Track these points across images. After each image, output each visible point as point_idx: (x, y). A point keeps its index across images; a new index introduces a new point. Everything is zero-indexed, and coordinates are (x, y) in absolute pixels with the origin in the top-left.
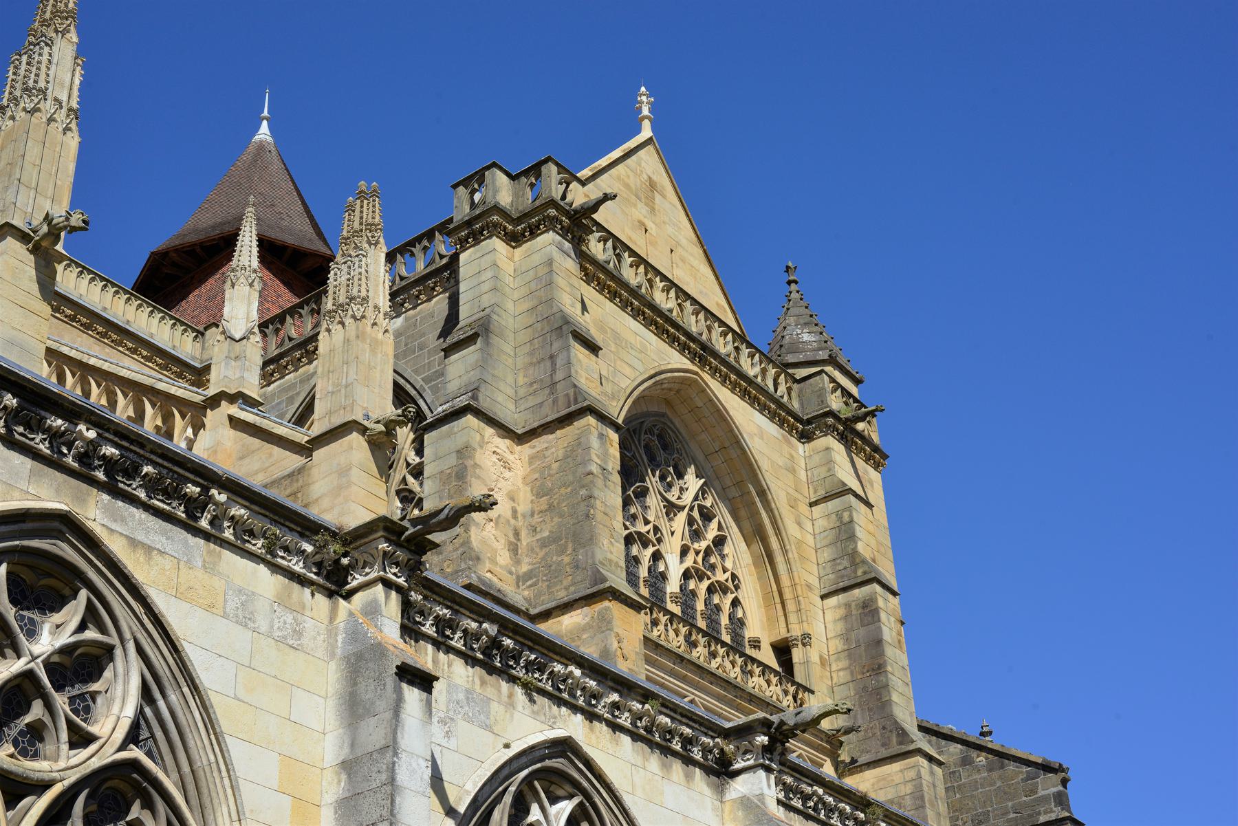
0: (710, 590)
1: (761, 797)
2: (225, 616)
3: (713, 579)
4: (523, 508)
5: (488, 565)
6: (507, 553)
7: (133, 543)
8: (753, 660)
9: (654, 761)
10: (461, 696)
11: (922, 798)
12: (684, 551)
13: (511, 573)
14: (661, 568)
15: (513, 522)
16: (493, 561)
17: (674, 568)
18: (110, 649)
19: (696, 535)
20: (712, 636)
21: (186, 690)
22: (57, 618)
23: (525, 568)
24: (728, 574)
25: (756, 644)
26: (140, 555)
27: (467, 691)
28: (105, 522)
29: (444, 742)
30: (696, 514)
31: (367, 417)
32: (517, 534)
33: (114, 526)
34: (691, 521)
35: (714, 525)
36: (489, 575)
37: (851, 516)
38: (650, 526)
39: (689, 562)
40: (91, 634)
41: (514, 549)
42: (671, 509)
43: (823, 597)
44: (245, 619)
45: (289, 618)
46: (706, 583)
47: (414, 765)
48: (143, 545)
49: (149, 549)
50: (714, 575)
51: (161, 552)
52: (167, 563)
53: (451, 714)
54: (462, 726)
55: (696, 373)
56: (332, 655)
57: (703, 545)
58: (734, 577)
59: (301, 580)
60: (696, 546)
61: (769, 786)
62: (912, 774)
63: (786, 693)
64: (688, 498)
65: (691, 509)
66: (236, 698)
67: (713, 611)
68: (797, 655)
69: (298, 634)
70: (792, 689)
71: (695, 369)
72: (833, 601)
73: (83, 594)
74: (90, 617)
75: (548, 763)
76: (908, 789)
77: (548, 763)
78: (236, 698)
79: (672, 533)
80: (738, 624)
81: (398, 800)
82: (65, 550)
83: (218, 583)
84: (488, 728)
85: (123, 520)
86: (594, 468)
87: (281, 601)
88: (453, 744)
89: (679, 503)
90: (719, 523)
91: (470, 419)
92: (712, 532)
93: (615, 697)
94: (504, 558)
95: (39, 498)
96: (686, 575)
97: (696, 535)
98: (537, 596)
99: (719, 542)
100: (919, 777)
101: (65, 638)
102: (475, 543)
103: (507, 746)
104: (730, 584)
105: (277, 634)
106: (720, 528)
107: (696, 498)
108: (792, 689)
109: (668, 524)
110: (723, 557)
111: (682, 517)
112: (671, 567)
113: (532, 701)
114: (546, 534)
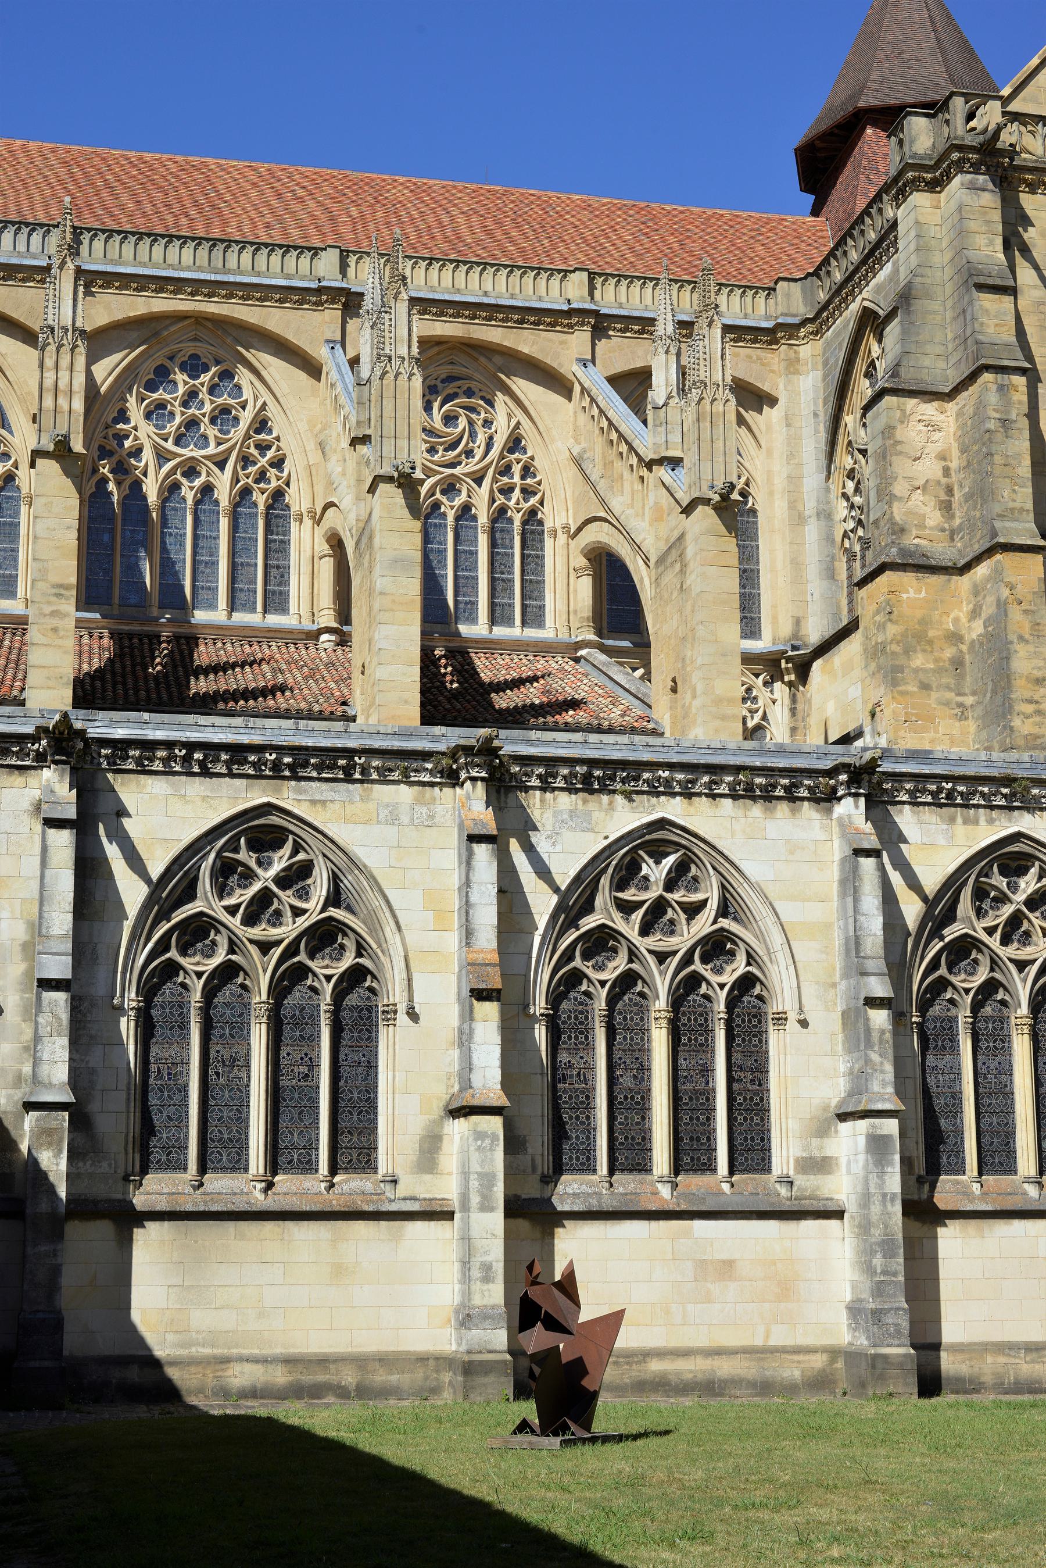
2: (379, 823)
5: (914, 532)
6: (938, 513)
7: (313, 802)
9: (756, 810)
10: (565, 816)
13: (943, 530)
15: (944, 481)
16: (922, 526)
18: (312, 861)
21: (356, 872)
22: (281, 852)
23: (957, 521)
26: (319, 807)
27: (571, 811)
28: (295, 797)
29: (551, 850)
33: (300, 797)
36: (917, 541)
40: (301, 856)
41: (946, 507)
44: (393, 819)
45: (424, 810)
48: (320, 801)
49: (323, 803)
52: (337, 806)
53: (557, 830)
54: (567, 835)
59: (432, 785)
66: (390, 867)
69: (431, 817)
73: (291, 837)
74: (296, 849)
75: (647, 837)
77: (647, 837)
78: (390, 867)
82: (275, 820)
83: (372, 806)
85: (306, 791)
87: (418, 801)
88: (559, 848)
93: (706, 779)
94: (934, 518)
95: (254, 799)
98: (965, 547)
101: (284, 864)
102: (898, 518)
103: (606, 838)
105: (416, 821)
113: (631, 800)
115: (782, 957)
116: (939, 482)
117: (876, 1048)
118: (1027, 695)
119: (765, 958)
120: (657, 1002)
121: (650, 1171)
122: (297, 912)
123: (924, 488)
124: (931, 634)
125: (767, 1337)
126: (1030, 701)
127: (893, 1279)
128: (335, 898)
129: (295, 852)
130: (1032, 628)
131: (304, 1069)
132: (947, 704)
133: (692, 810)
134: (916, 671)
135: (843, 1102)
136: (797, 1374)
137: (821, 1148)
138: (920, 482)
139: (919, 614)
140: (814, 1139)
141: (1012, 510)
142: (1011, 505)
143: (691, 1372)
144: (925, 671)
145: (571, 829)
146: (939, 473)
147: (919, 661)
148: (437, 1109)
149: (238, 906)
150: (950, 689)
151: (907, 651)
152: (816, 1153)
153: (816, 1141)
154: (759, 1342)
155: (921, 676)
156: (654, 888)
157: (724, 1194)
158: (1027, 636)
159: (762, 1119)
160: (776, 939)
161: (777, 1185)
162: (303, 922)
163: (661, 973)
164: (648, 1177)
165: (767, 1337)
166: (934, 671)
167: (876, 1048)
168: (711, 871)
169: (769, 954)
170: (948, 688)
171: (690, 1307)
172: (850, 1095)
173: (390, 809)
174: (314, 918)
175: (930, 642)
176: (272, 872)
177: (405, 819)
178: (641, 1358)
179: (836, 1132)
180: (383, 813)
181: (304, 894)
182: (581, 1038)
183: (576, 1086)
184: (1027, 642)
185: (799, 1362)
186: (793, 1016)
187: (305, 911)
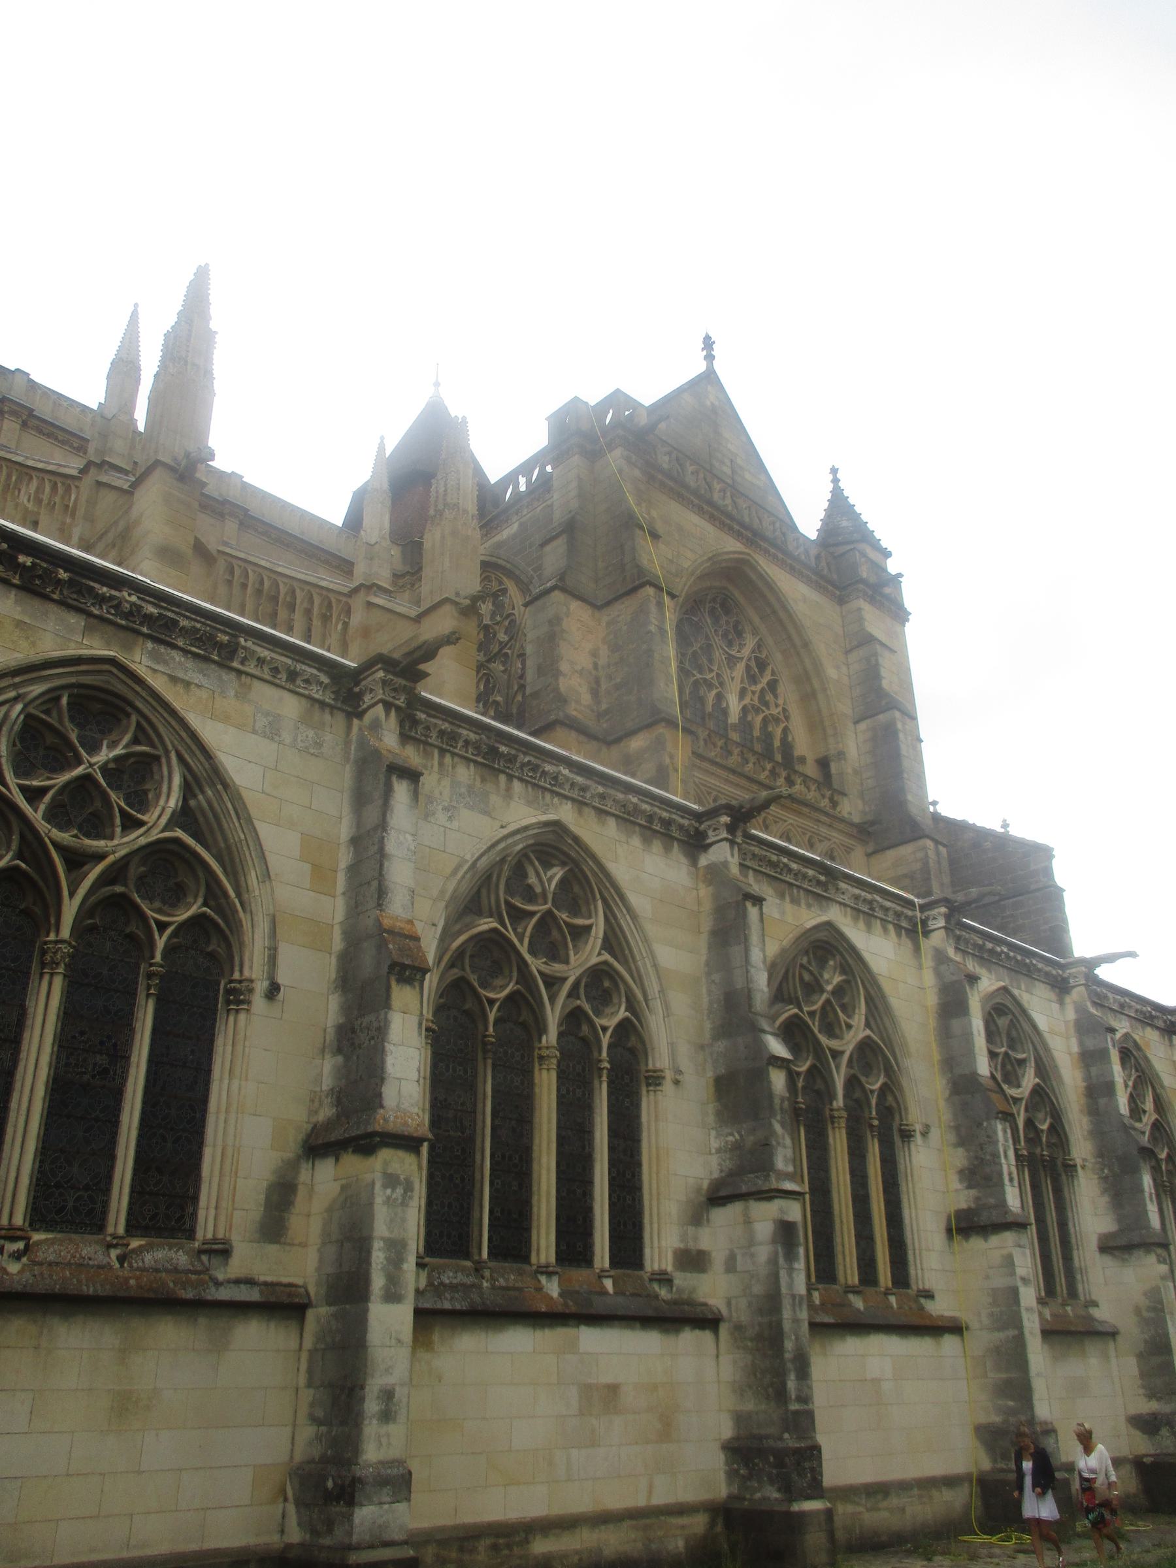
0: (765, 721)
1: (725, 864)
3: (767, 712)
4: (602, 661)
5: (573, 705)
7: (174, 679)
8: (796, 772)
10: (463, 790)
11: (929, 873)
12: (742, 693)
14: (724, 705)
15: (594, 672)
16: (578, 702)
17: (734, 705)
18: (157, 758)
19: (753, 679)
20: (768, 754)
21: (219, 787)
23: (604, 707)
24: (780, 709)
25: (802, 760)
26: (180, 688)
28: (150, 664)
29: (448, 824)
30: (753, 664)
31: (457, 594)
32: (597, 681)
33: (157, 667)
34: (748, 667)
35: (768, 672)
36: (574, 713)
37: (877, 661)
38: (714, 674)
39: (747, 701)
41: (595, 693)
42: (732, 661)
43: (856, 723)
44: (272, 732)
45: (311, 733)
46: (761, 717)
47: (401, 838)
48: (183, 681)
49: (187, 684)
50: (768, 708)
51: (198, 686)
52: (204, 694)
53: (454, 803)
54: (465, 813)
55: (749, 554)
56: (347, 760)
57: (759, 687)
58: (784, 710)
59: (322, 704)
60: (753, 688)
61: (733, 855)
62: (920, 855)
63: (823, 796)
64: (746, 652)
65: (749, 659)
66: (263, 792)
67: (767, 737)
68: (834, 768)
70: (828, 793)
71: (747, 551)
72: (863, 726)
73: (134, 718)
76: (918, 865)
78: (263, 792)
79: (733, 679)
80: (787, 747)
81: (386, 864)
84: (486, 813)
85: (165, 662)
86: (653, 628)
88: (455, 825)
89: (738, 655)
90: (773, 671)
91: (556, 593)
92: (767, 677)
94: (586, 698)
95: (92, 648)
96: (745, 710)
97: (753, 679)
99: (773, 686)
100: (927, 856)
102: (562, 688)
103: (502, 827)
104: (781, 717)
106: (773, 673)
107: (753, 651)
108: (828, 793)
109: (728, 671)
110: (776, 696)
111: (740, 668)
112: (731, 706)
114: (618, 680)
115: (657, 1004)
117: (779, 1118)
120: (544, 1038)
121: (526, 1259)
122: (131, 823)
123: (581, 673)
125: (650, 1492)
127: (806, 1407)
128: (185, 817)
129: (136, 741)
131: (102, 1060)
135: (716, 1185)
136: (681, 1544)
137: (696, 1239)
138: (578, 667)
140: (689, 1227)
143: (577, 1552)
146: (591, 666)
148: (292, 1147)
149: (43, 791)
152: (691, 1245)
153: (691, 1230)
154: (641, 1502)
156: (540, 901)
157: (606, 1293)
159: (634, 1200)
160: (653, 987)
161: (656, 1286)
162: (138, 839)
163: (552, 999)
164: (526, 1267)
165: (650, 1492)
167: (779, 1118)
168: (598, 896)
169: (646, 1000)
171: (574, 1452)
172: (733, 1175)
173: (270, 719)
174: (155, 835)
176: (104, 755)
177: (287, 737)
178: (523, 1535)
179: (708, 1220)
180: (262, 722)
181: (141, 801)
183: (452, 1133)
185: (683, 1527)
186: (669, 1075)
187: (141, 824)
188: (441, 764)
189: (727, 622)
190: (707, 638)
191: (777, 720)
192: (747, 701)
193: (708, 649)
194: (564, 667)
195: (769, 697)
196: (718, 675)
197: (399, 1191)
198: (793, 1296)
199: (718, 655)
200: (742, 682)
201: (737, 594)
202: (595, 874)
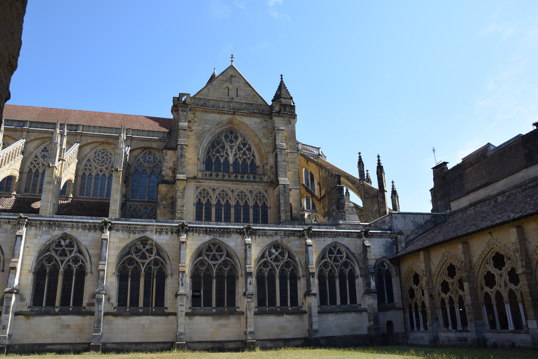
0: (245, 160)
2: (2, 233)
5: (166, 177)
13: (173, 177)
17: (231, 159)
45: (13, 230)
55: (233, 118)
71: (232, 117)
111: (235, 148)
116: (173, 167)
118: (179, 209)
119: (85, 261)
124: (167, 197)
126: (180, 210)
130: (182, 196)
132: (169, 211)
133: (72, 231)
134: (163, 204)
139: (165, 193)
141: (181, 172)
142: (181, 171)
144: (165, 205)
145: (45, 234)
147: (164, 202)
150: (170, 208)
151: (161, 201)
155: (164, 206)
158: (181, 197)
166: (167, 204)
170: (170, 208)
175: (167, 199)
177: (8, 232)
180: (4, 231)
182: (43, 277)
184: (181, 198)
188: (39, 228)
189: (231, 137)
190: (223, 143)
191: (249, 158)
192: (237, 156)
193: (223, 147)
194: (164, 168)
195: (247, 152)
196: (226, 153)
197: (9, 299)
198: (98, 311)
199: (227, 147)
200: (236, 151)
201: (235, 127)
202: (74, 239)
